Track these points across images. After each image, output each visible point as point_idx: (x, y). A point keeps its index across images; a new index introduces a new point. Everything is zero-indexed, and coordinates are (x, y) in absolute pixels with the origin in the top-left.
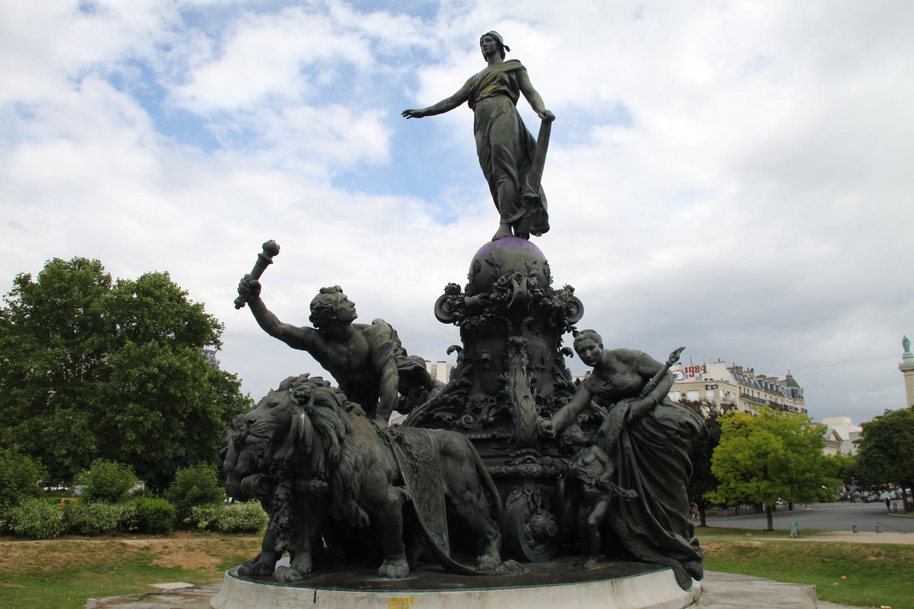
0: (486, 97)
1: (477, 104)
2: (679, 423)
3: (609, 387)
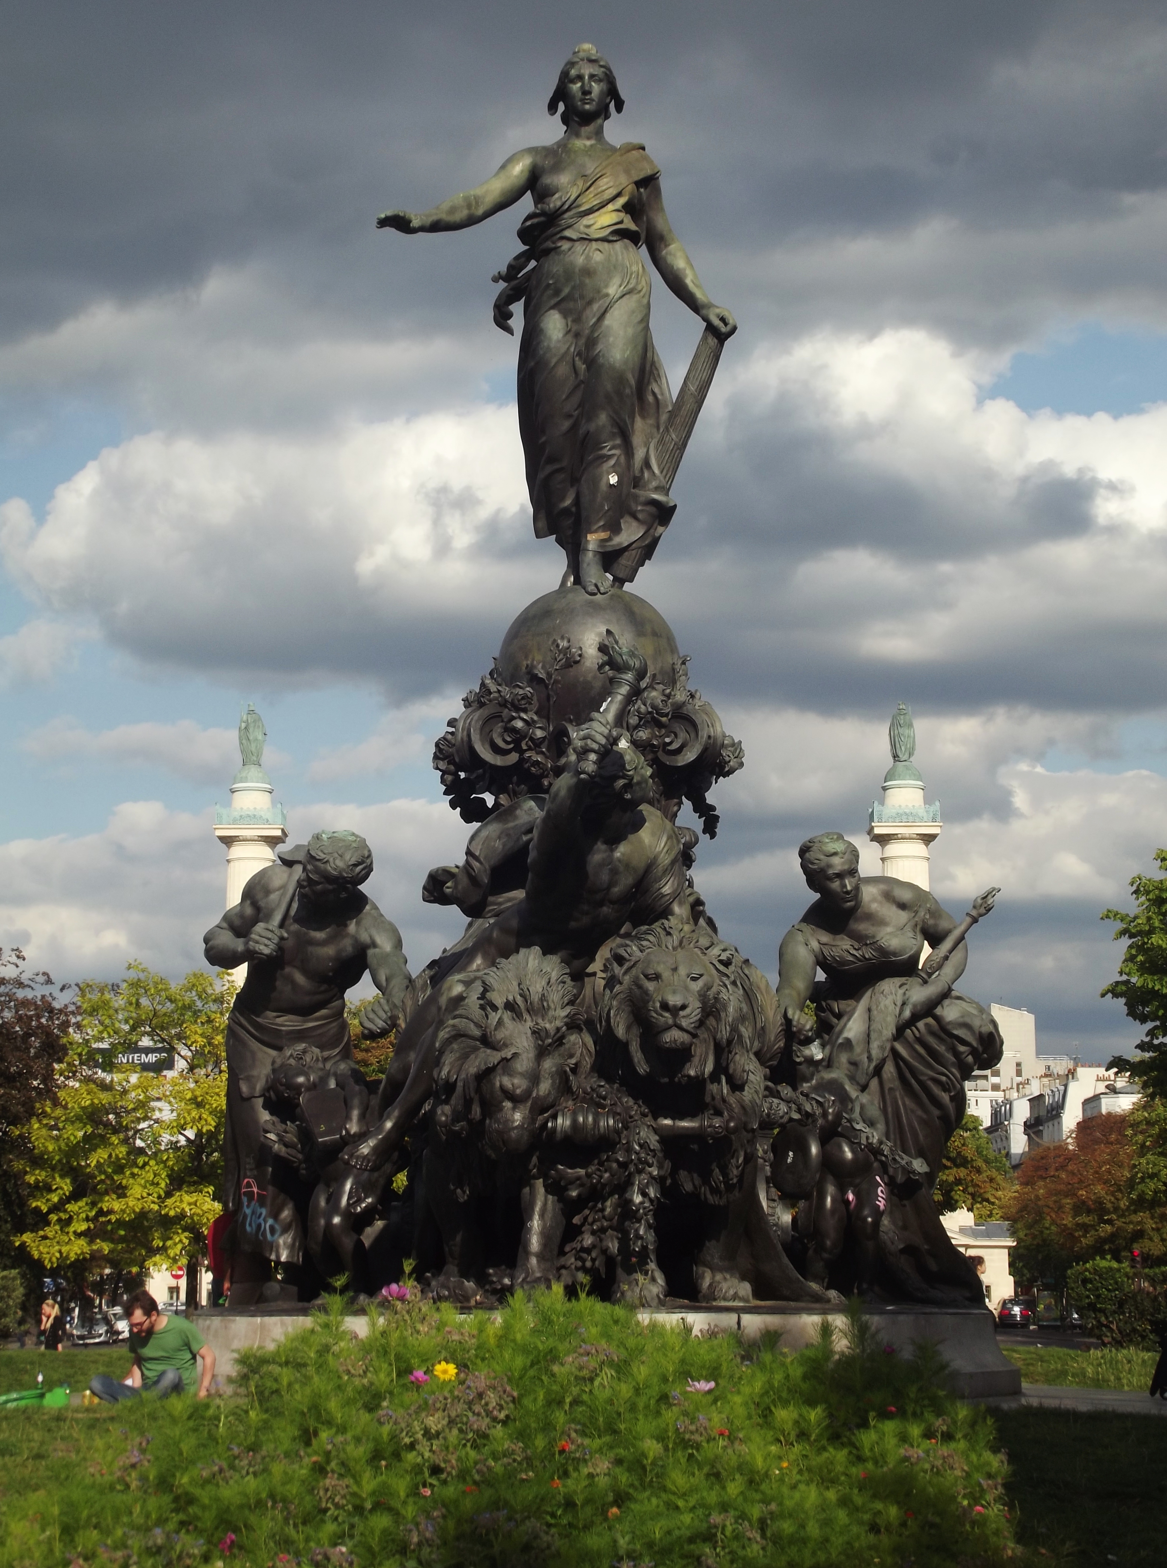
0: (597, 240)
1: (565, 246)
2: (980, 1033)
3: (868, 953)
